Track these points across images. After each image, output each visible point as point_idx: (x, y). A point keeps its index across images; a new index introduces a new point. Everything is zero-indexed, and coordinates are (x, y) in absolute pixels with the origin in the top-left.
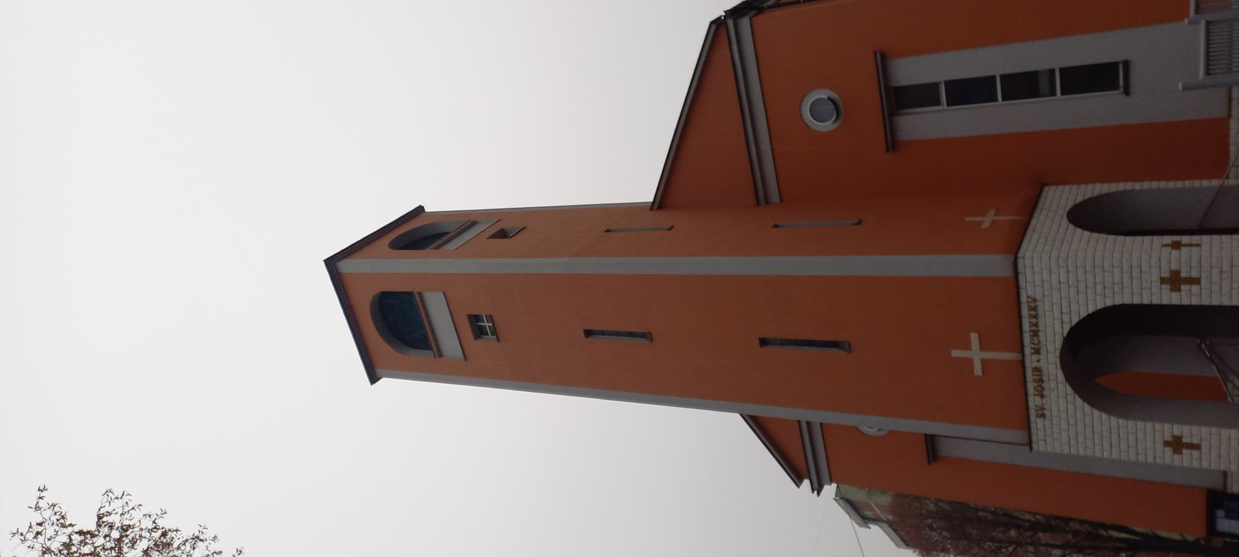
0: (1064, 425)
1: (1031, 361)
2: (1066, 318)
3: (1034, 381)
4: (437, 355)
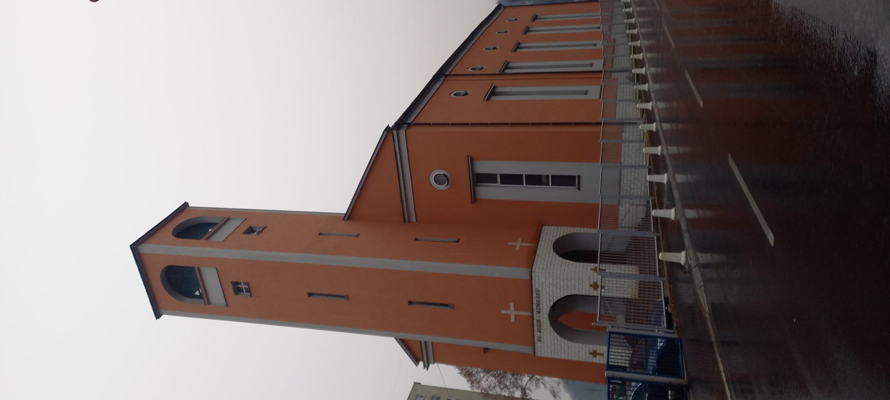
0: (549, 345)
1: (536, 317)
2: (551, 299)
3: (537, 325)
4: (207, 303)
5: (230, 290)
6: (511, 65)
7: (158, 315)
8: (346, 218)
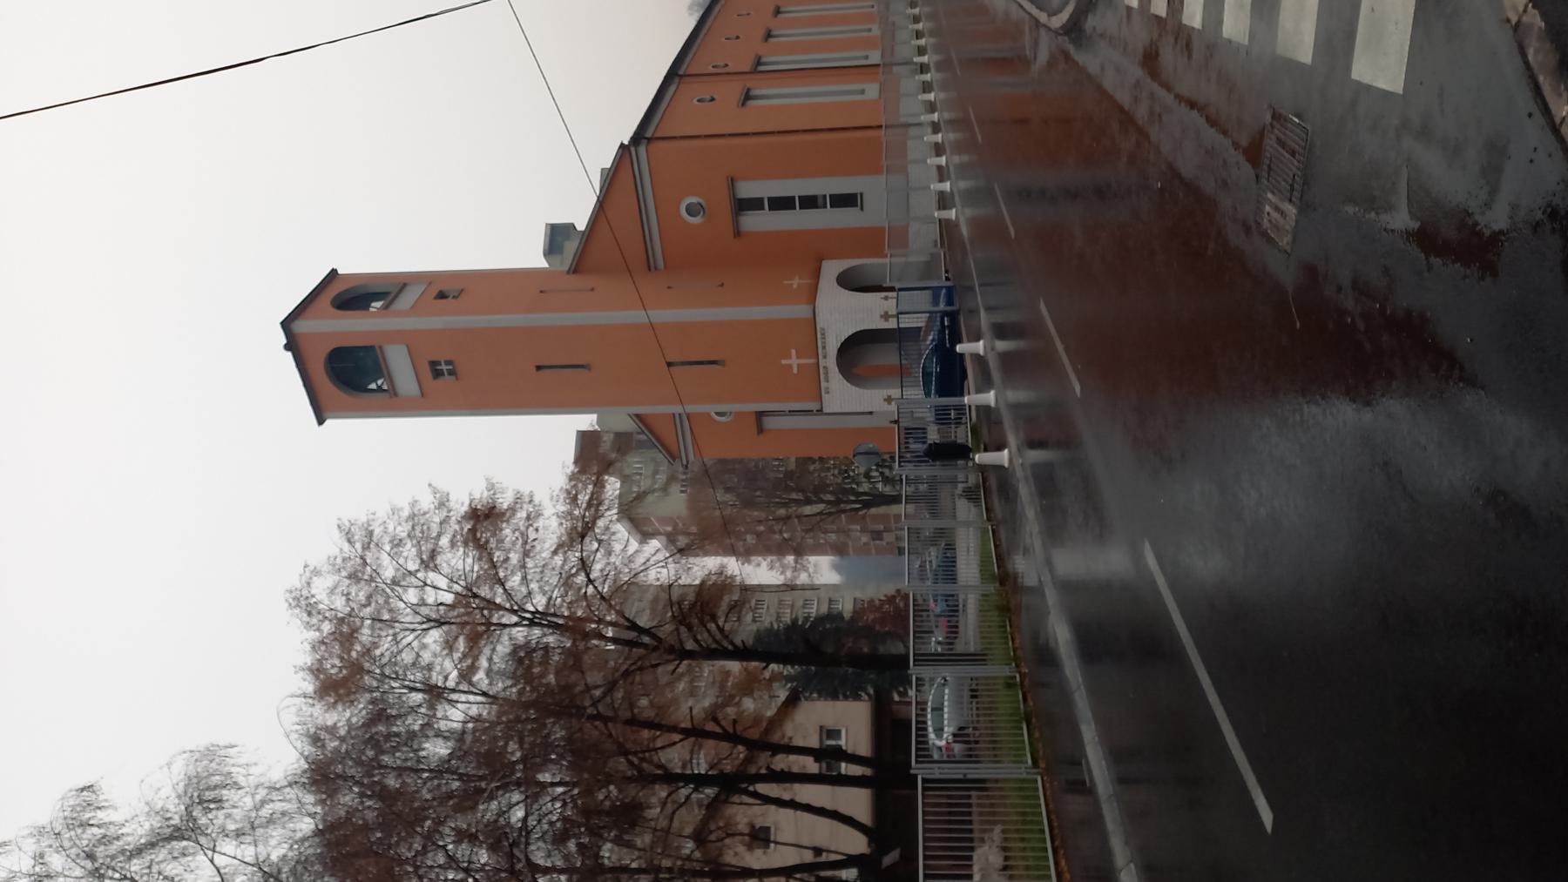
1: (822, 362)
2: (839, 338)
5: (427, 372)
6: (764, 60)
7: (321, 422)
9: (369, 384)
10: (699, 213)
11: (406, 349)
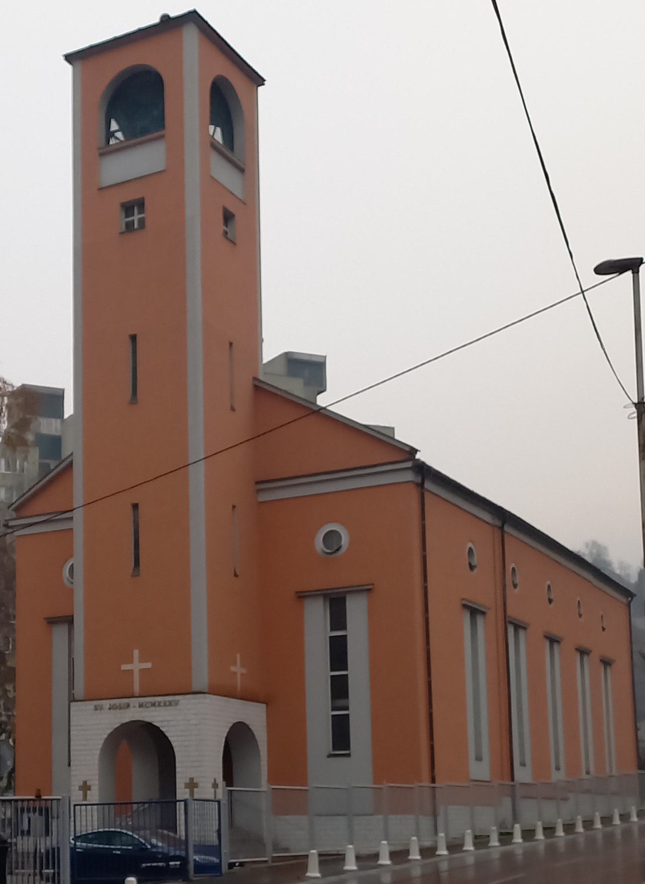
1: (134, 702)
5: (130, 195)
7: (70, 58)
8: (257, 383)
9: (117, 121)
10: (328, 549)
11: (162, 169)
